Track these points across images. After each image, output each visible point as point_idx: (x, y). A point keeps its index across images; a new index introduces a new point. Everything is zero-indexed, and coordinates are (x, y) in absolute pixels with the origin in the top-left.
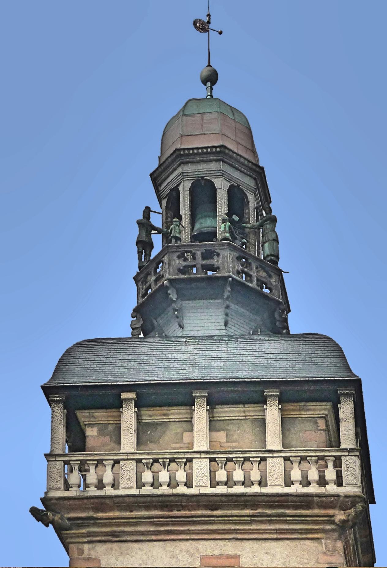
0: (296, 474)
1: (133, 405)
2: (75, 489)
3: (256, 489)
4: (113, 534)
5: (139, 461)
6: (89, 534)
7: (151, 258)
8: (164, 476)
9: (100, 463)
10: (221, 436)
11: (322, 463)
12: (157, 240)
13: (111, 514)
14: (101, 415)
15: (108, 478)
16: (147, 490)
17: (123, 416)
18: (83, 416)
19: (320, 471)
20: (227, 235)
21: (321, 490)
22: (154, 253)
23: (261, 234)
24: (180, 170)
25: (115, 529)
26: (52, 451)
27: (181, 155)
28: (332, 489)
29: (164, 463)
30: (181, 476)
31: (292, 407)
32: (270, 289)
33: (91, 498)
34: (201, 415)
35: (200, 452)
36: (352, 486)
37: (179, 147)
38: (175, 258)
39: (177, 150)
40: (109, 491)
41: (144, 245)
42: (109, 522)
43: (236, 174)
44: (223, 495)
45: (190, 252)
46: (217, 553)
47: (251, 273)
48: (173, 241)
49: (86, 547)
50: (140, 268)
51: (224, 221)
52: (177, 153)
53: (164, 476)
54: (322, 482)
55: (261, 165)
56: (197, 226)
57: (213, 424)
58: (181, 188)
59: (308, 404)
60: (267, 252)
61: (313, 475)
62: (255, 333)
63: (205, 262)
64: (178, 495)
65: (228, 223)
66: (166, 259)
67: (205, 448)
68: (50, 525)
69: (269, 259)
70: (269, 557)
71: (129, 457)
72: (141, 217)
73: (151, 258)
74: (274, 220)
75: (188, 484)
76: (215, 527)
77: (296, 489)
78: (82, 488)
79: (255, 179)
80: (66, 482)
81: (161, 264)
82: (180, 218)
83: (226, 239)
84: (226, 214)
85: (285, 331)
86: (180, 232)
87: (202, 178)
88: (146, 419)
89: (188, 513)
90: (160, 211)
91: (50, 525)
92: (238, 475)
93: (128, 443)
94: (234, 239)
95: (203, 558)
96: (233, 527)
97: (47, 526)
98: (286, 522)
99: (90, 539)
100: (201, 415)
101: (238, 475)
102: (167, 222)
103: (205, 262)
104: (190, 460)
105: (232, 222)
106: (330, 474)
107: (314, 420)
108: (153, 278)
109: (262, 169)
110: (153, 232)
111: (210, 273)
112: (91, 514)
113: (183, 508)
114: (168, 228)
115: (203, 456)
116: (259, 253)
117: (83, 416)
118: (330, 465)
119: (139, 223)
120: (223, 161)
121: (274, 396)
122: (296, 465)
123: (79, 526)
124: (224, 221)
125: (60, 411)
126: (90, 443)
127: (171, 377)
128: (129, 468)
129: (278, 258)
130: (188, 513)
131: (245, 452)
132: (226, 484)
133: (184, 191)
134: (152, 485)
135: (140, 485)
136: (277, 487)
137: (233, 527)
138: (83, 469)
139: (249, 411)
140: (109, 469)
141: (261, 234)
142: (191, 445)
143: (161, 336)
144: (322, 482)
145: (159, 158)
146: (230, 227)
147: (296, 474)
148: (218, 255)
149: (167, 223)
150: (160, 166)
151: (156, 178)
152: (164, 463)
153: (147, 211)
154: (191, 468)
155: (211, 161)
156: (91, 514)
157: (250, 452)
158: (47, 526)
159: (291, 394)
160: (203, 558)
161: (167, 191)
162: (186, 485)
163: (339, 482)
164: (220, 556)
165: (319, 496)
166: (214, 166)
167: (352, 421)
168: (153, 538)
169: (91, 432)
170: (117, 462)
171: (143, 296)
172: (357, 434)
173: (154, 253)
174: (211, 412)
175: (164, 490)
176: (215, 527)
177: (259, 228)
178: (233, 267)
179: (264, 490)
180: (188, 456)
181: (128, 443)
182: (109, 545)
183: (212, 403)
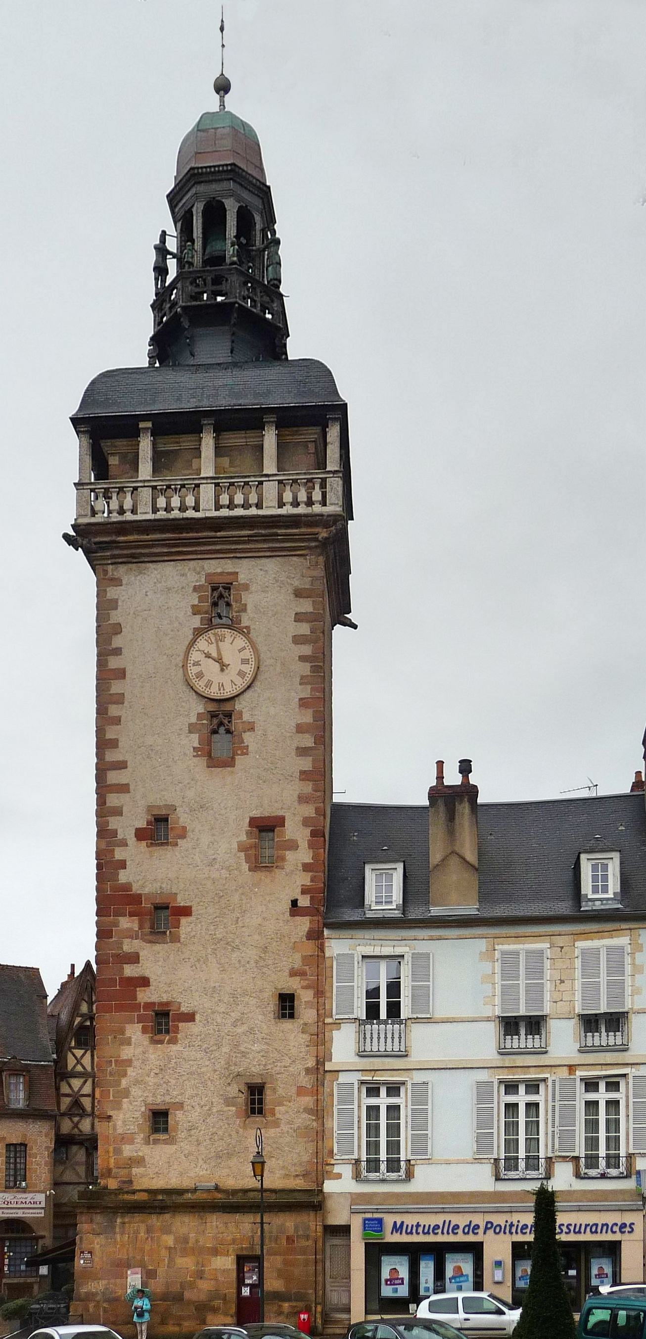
0: (288, 496)
1: (149, 434)
2: (100, 515)
3: (253, 511)
4: (133, 556)
5: (154, 488)
6: (113, 557)
7: (167, 284)
8: (176, 502)
9: (121, 490)
10: (225, 461)
11: (311, 484)
12: (172, 265)
13: (131, 538)
14: (122, 444)
15: (128, 503)
16: (161, 515)
17: (141, 444)
18: (106, 445)
19: (308, 493)
20: (235, 259)
21: (308, 510)
22: (170, 279)
23: (266, 257)
24: (193, 191)
25: (134, 551)
26: (80, 480)
27: (194, 175)
28: (317, 509)
29: (176, 489)
30: (190, 501)
31: (287, 433)
32: (273, 315)
33: (114, 523)
34: (208, 442)
35: (207, 478)
36: (334, 507)
37: (193, 165)
38: (188, 284)
39: (192, 169)
40: (129, 516)
41: (161, 270)
42: (128, 545)
43: (246, 195)
44: (225, 518)
45: (201, 277)
46: (219, 570)
47: (256, 299)
48: (187, 266)
49: (110, 567)
50: (156, 295)
51: (233, 245)
52: (192, 172)
53: (176, 502)
54: (310, 503)
55: (268, 184)
56: (207, 252)
57: (219, 451)
58: (194, 210)
59: (301, 428)
60: (271, 276)
61: (302, 496)
62: (257, 360)
63: (214, 288)
64: (187, 519)
65: (236, 247)
66: (179, 285)
67: (211, 474)
68: (80, 549)
69: (272, 283)
70: (262, 572)
71: (146, 484)
72: (158, 242)
73: (167, 284)
74: (278, 242)
75: (196, 508)
76: (218, 547)
77: (288, 510)
78: (106, 515)
79: (262, 198)
80: (92, 508)
81: (175, 291)
82: (193, 241)
83: (233, 263)
84: (235, 237)
85: (284, 357)
86: (193, 257)
87: (214, 198)
88: (162, 448)
89: (195, 535)
90: (175, 235)
91: (80, 549)
92: (239, 499)
93: (145, 470)
94: (241, 262)
95: (208, 575)
96: (233, 547)
97: (77, 550)
98: (278, 541)
99: (114, 561)
100: (208, 442)
101: (239, 499)
102: (181, 246)
103: (214, 288)
104: (198, 486)
105: (240, 245)
106: (317, 495)
107: (305, 445)
108: (168, 305)
109: (269, 187)
110: (168, 256)
111: (219, 299)
112: (114, 538)
113: (191, 530)
114: (182, 252)
115: (209, 481)
116: (263, 277)
117: (106, 445)
118: (317, 487)
119: (156, 247)
120: (235, 181)
121: (272, 422)
122: (288, 488)
123: (103, 549)
124: (233, 245)
125: (86, 440)
126: (112, 471)
127: (183, 406)
128: (146, 494)
129: (280, 282)
130: (195, 535)
131: (246, 477)
132: (228, 507)
133: (197, 213)
134: (166, 510)
135: (155, 510)
136: (270, 509)
137: (233, 547)
138: (107, 497)
139: (250, 437)
140: (129, 495)
141: (266, 257)
142: (199, 471)
143: (174, 365)
144: (310, 503)
145: (175, 177)
146: (238, 251)
147: (288, 496)
148: (227, 280)
149: (181, 247)
150: (175, 186)
151: (173, 199)
152: (176, 489)
153: (164, 234)
154: (199, 493)
155: (222, 180)
156: (114, 538)
157: (249, 476)
158: (77, 550)
159: (290, 420)
160: (208, 575)
161: (182, 212)
162: (194, 509)
163: (324, 503)
164: (221, 574)
165: (306, 516)
166: (225, 185)
167: (337, 444)
168: (166, 558)
169: (113, 461)
170: (135, 488)
171: (159, 324)
172: (341, 456)
173: (170, 279)
174: (217, 439)
175: (176, 514)
176: (218, 547)
177: (264, 251)
178: (240, 293)
179: (260, 512)
180: (197, 482)
181: (145, 470)
182: (130, 565)
183: (218, 430)
